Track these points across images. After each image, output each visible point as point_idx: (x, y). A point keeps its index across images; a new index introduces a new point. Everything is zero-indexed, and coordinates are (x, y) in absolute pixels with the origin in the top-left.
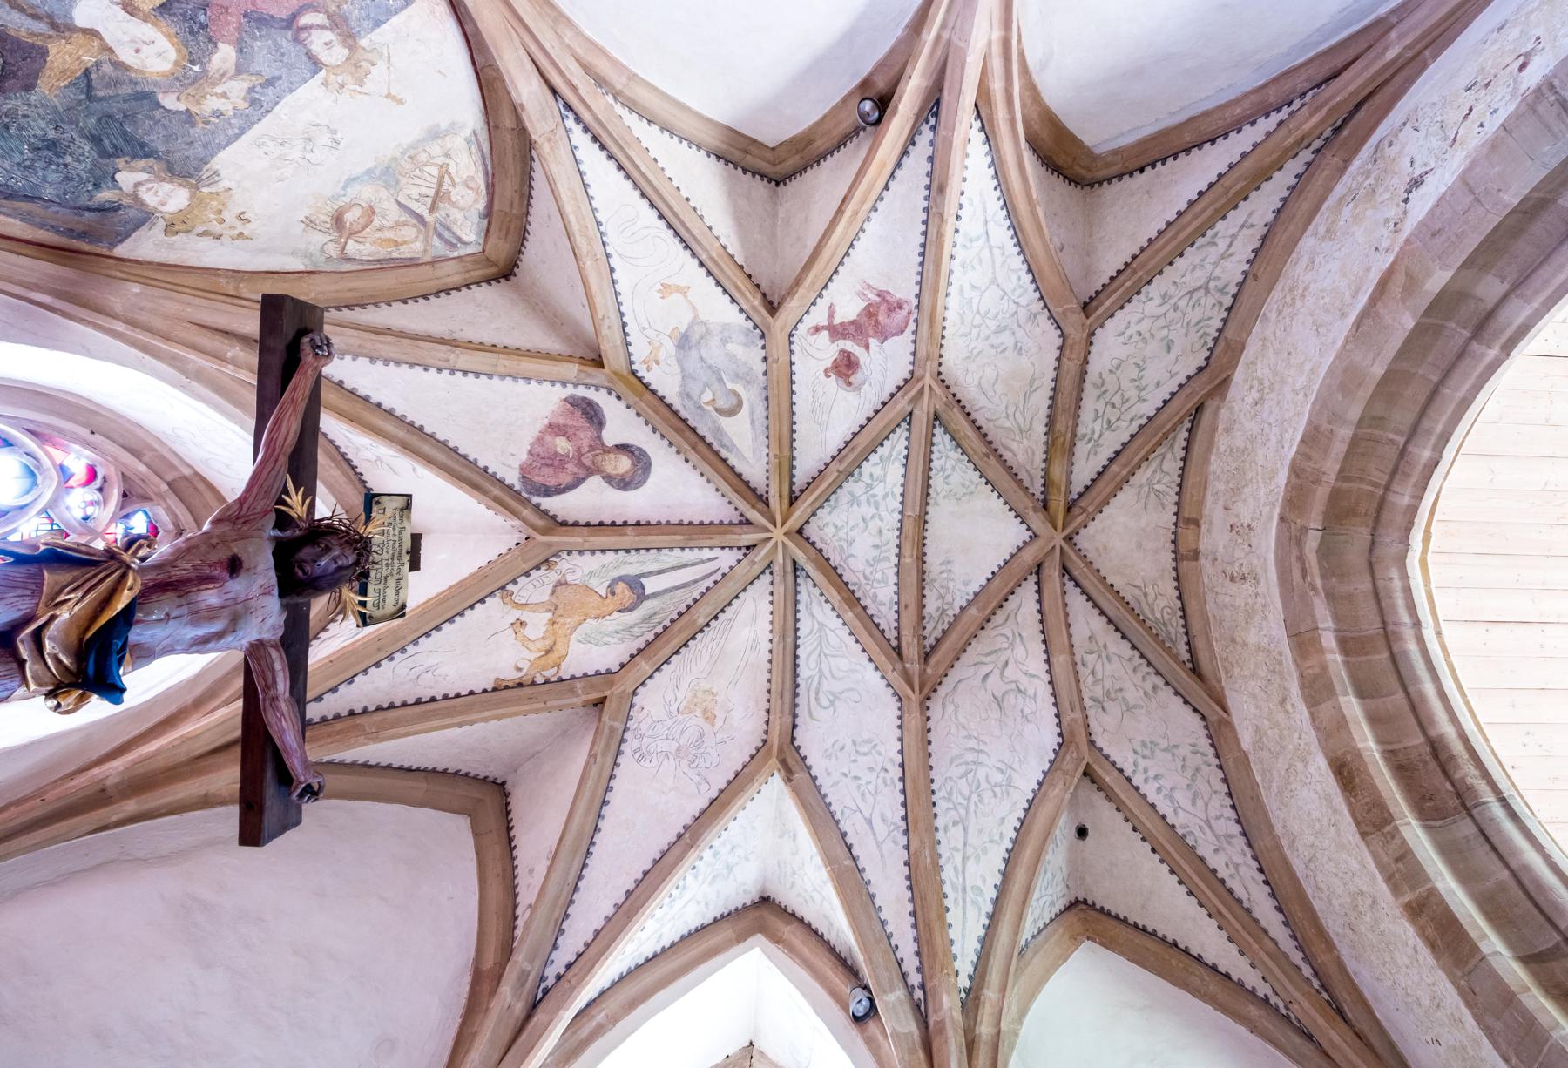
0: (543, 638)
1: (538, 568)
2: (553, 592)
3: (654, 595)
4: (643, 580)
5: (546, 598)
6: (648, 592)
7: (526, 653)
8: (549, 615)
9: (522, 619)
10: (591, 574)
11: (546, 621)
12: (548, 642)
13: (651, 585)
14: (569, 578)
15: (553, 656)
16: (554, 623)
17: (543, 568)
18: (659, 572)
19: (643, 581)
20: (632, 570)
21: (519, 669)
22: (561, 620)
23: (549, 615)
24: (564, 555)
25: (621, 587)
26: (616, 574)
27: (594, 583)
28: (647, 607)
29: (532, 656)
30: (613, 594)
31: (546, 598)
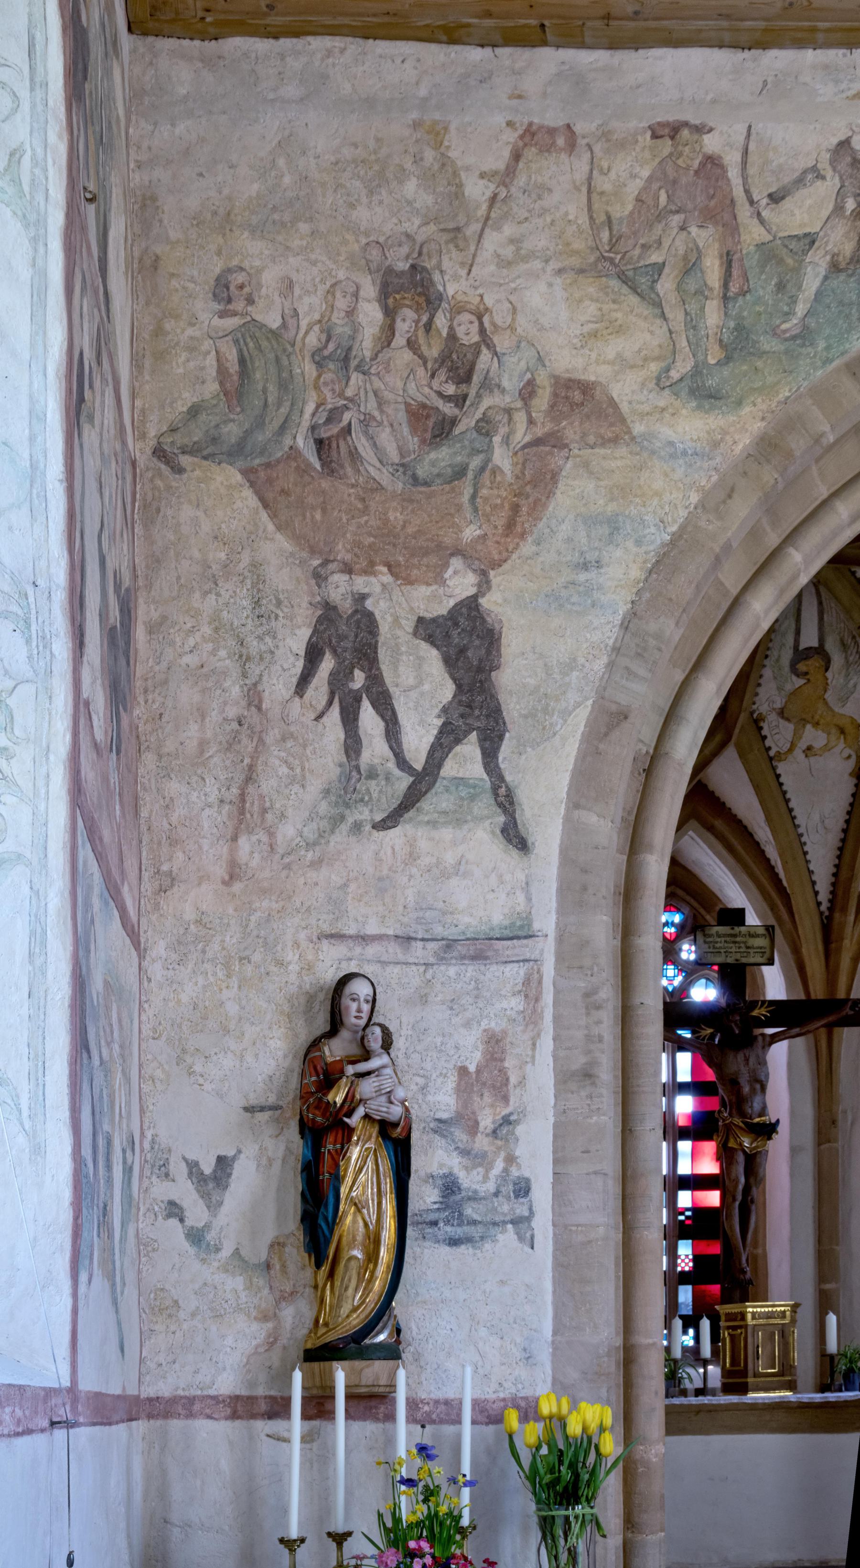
0: (829, 734)
1: (761, 728)
2: (788, 720)
3: (822, 640)
4: (802, 647)
5: (791, 727)
6: (815, 644)
7: (837, 750)
8: (809, 727)
9: (804, 747)
10: (780, 689)
11: (812, 730)
12: (834, 731)
13: (809, 639)
14: (778, 705)
15: (849, 729)
16: (818, 724)
17: (762, 724)
18: (798, 632)
19: (802, 647)
20: (787, 656)
21: (849, 757)
22: (817, 717)
23: (809, 727)
24: (755, 707)
25: (802, 667)
26: (787, 669)
27: (789, 687)
28: (831, 646)
29: (842, 745)
30: (806, 673)
31: (791, 727)
